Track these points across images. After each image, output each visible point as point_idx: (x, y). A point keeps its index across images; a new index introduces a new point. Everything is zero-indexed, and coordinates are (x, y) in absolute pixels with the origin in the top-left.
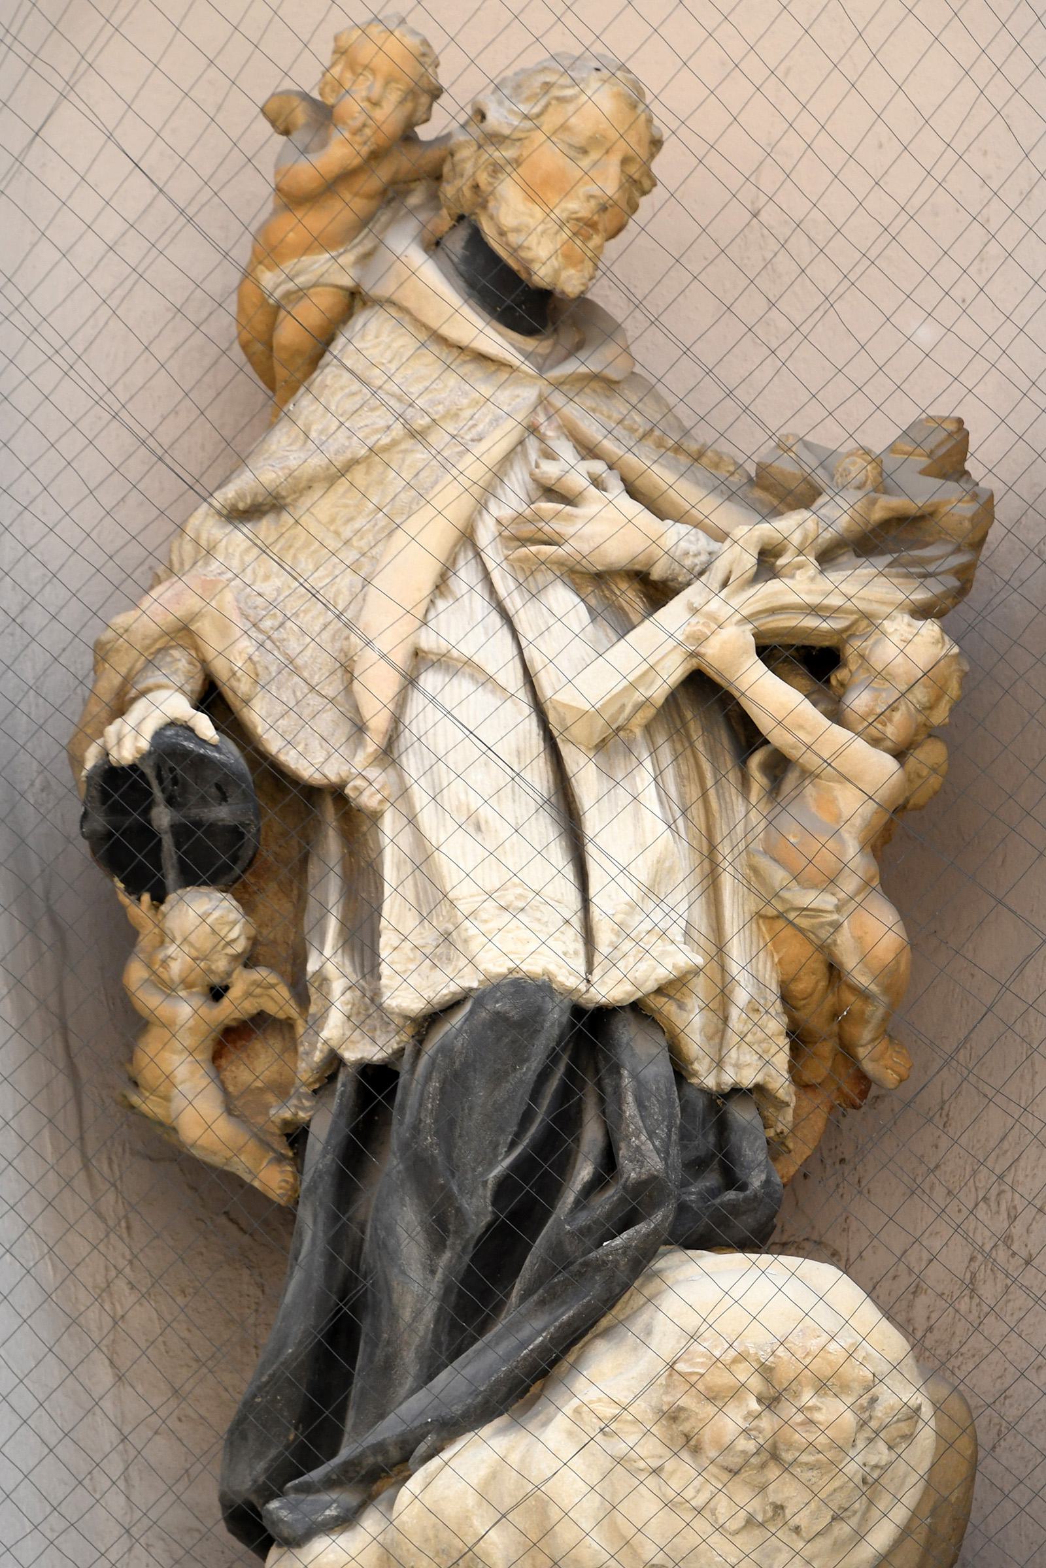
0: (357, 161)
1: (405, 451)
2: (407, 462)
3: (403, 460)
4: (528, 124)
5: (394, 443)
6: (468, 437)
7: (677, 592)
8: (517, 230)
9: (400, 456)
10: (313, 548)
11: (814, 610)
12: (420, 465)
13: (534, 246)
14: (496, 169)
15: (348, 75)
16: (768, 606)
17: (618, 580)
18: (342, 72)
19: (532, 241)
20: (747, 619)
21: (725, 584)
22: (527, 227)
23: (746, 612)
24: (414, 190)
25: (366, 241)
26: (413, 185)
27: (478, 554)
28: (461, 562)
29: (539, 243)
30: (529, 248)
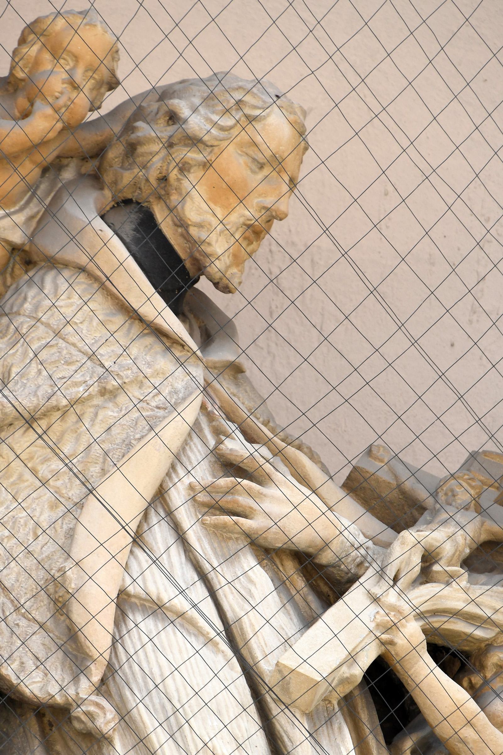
0: (51, 135)
1: (97, 406)
2: (100, 417)
3: (96, 415)
4: (222, 134)
5: (90, 397)
6: (154, 404)
7: (353, 579)
8: (200, 226)
9: (92, 410)
10: (12, 480)
11: (470, 618)
12: (112, 421)
13: (213, 243)
14: (184, 168)
15: (47, 56)
16: (434, 607)
17: (284, 557)
18: (40, 51)
19: (213, 238)
20: (420, 616)
21: (396, 579)
22: (210, 224)
23: (422, 608)
24: (67, 165)
25: (31, 205)
26: (65, 161)
27: (170, 514)
28: (154, 519)
29: (217, 241)
30: (209, 244)
